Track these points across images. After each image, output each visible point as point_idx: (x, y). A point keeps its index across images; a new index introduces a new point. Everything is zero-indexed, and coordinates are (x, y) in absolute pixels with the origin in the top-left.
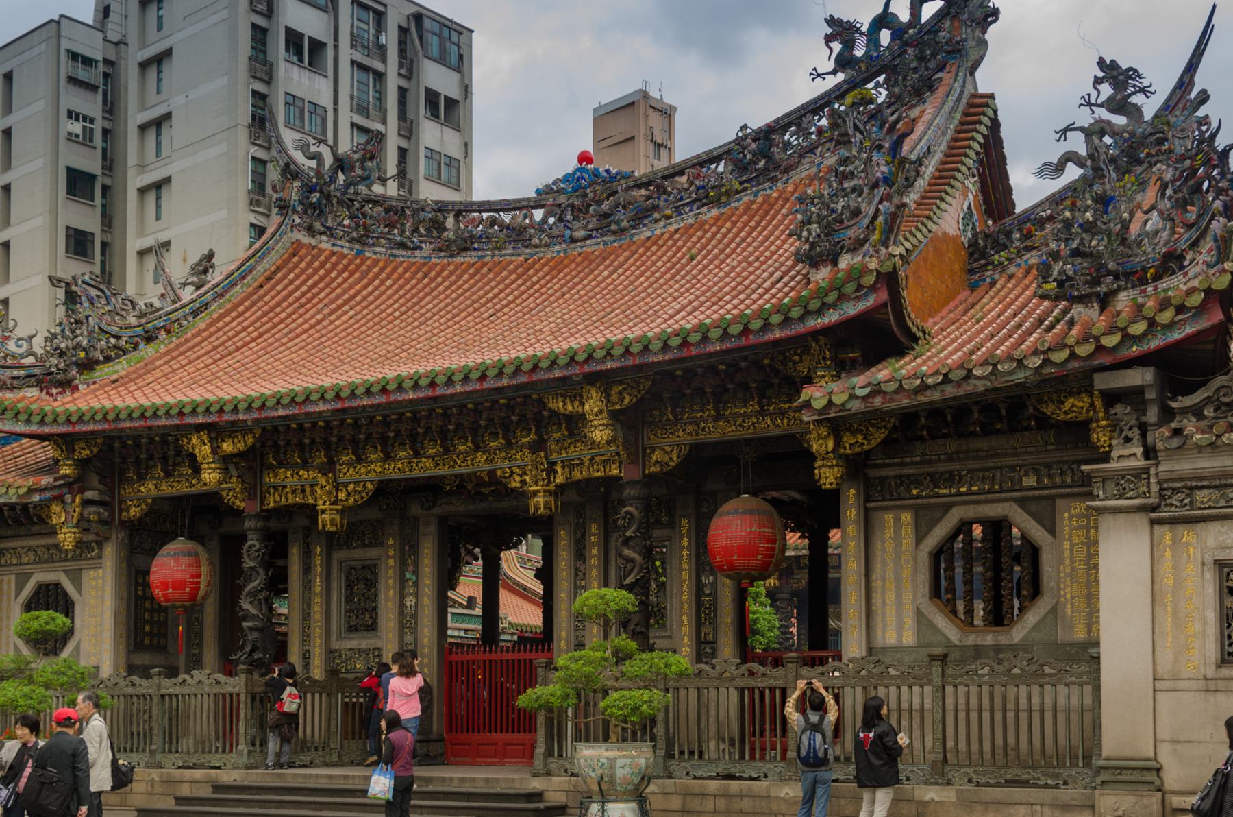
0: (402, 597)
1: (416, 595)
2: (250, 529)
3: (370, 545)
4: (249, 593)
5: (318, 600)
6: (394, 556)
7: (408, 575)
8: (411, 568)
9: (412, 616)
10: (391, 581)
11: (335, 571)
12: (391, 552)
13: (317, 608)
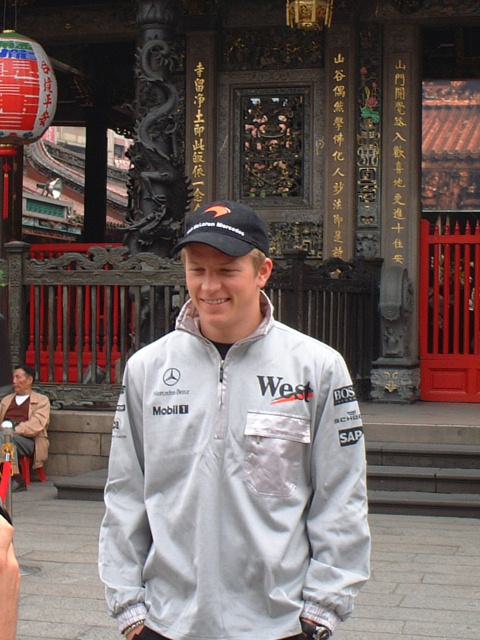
0: (356, 146)
1: (380, 143)
2: (154, 21)
3: (294, 64)
4: (154, 123)
5: (199, 145)
6: (343, 82)
7: (365, 113)
8: (370, 101)
9: (372, 175)
10: (339, 121)
11: (225, 103)
12: (339, 76)
13: (198, 158)
